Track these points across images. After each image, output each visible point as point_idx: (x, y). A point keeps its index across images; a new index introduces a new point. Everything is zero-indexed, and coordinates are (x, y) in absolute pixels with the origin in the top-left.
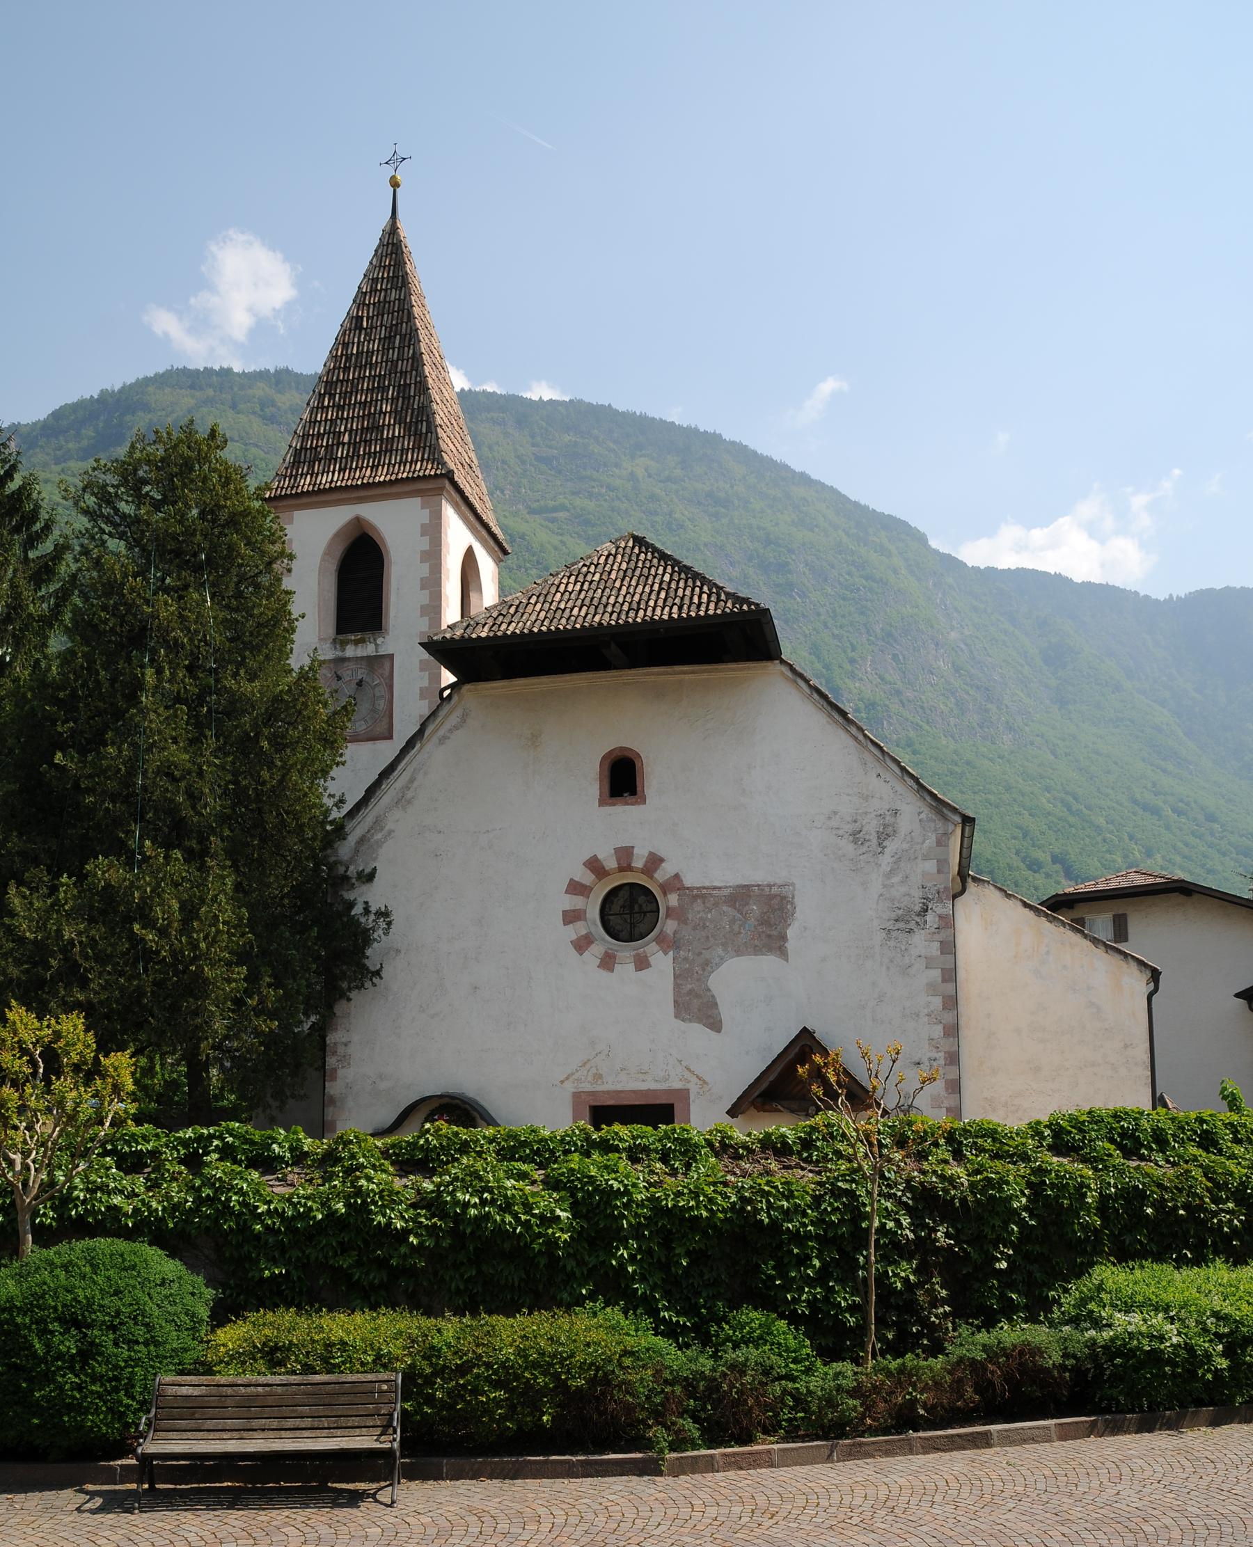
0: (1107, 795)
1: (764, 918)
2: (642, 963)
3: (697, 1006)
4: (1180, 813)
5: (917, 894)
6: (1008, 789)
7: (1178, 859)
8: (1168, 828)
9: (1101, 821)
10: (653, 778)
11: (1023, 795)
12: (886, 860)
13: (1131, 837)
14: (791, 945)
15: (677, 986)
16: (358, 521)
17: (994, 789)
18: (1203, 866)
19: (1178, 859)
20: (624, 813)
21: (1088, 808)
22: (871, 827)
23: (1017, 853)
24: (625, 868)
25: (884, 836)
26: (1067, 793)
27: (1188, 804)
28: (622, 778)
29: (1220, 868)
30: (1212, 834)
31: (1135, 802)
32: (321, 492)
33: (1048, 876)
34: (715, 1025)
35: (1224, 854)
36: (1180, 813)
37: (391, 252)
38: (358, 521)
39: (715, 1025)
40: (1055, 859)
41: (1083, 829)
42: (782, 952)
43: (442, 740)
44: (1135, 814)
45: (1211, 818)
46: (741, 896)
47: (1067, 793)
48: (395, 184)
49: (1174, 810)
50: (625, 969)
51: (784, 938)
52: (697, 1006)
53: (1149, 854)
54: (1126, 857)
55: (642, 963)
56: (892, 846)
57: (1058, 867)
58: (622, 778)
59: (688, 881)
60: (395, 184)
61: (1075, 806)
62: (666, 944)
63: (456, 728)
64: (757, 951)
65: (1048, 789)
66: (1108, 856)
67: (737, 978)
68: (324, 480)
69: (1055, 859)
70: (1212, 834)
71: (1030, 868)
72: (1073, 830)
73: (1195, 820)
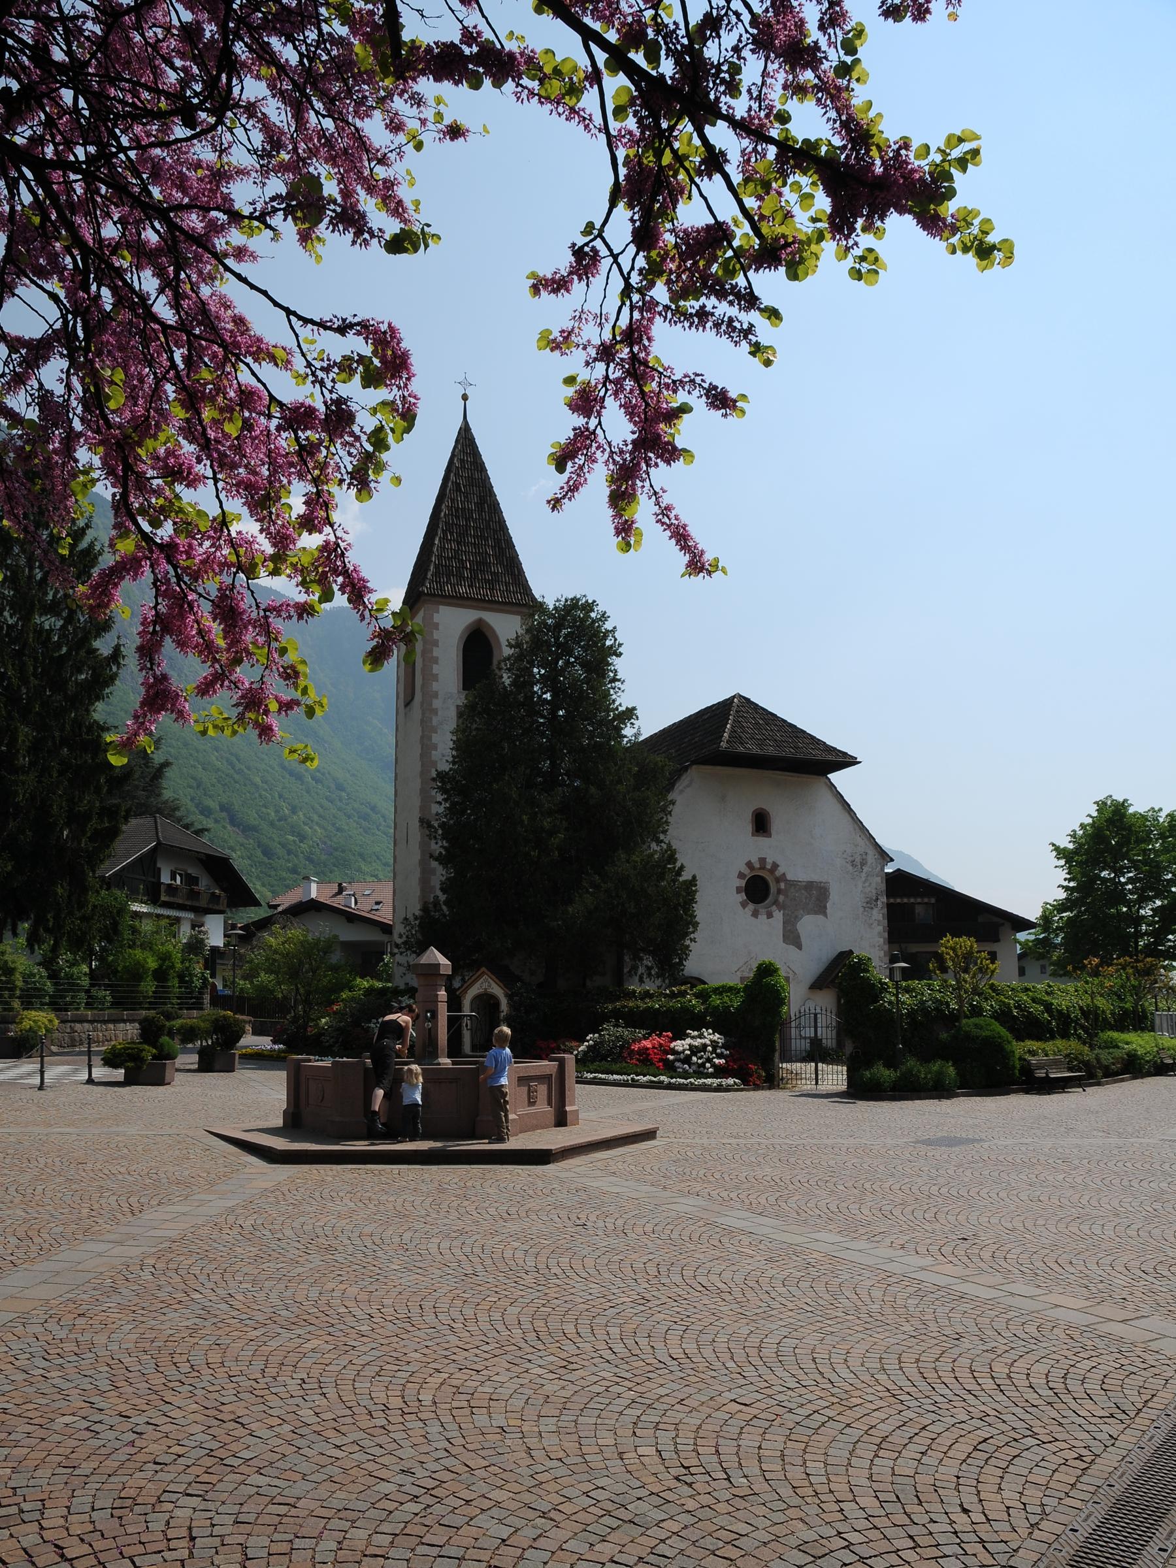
0: (262, 760)
1: (816, 897)
2: (770, 915)
3: (792, 938)
4: (317, 781)
5: (874, 891)
6: (186, 744)
7: (316, 818)
8: (308, 792)
9: (258, 780)
10: (776, 825)
11: (198, 752)
12: (863, 875)
13: (280, 796)
14: (828, 911)
15: (784, 928)
16: (480, 621)
17: (174, 743)
18: (334, 824)
19: (316, 818)
20: (762, 841)
21: (249, 768)
22: (858, 860)
23: (192, 799)
24: (763, 868)
25: (863, 864)
26: (231, 754)
27: (323, 774)
28: (761, 824)
29: (346, 828)
30: (341, 800)
31: (284, 768)
32: (462, 598)
33: (216, 821)
34: (799, 947)
35: (349, 817)
36: (317, 781)
37: (466, 442)
38: (480, 621)
39: (799, 947)
40: (223, 808)
41: (245, 785)
42: (825, 915)
43: (681, 792)
44: (283, 777)
45: (340, 788)
46: (810, 886)
47: (231, 754)
48: (465, 398)
49: (313, 778)
50: (763, 917)
51: (825, 907)
52: (792, 938)
53: (294, 810)
54: (277, 812)
55: (770, 915)
56: (866, 869)
57: (224, 814)
58: (761, 824)
59: (789, 877)
60: (465, 398)
61: (238, 766)
62: (781, 907)
63: (688, 786)
64: (816, 913)
65: (217, 749)
66: (264, 810)
67: (808, 924)
68: (462, 590)
69: (223, 808)
70: (341, 800)
71: (202, 813)
72: (238, 786)
73: (329, 788)
